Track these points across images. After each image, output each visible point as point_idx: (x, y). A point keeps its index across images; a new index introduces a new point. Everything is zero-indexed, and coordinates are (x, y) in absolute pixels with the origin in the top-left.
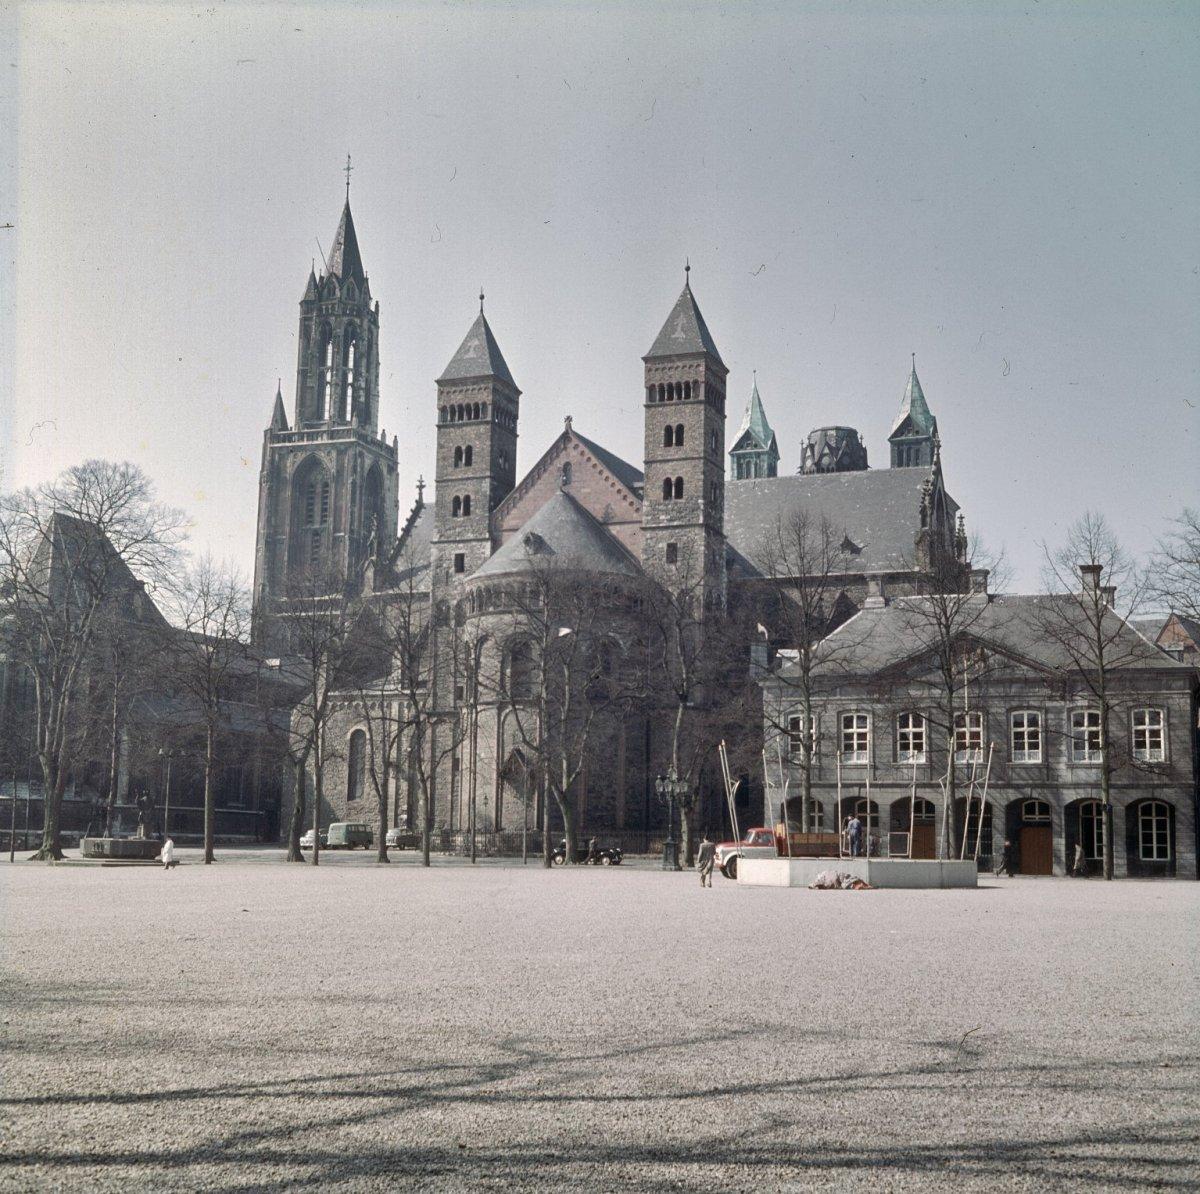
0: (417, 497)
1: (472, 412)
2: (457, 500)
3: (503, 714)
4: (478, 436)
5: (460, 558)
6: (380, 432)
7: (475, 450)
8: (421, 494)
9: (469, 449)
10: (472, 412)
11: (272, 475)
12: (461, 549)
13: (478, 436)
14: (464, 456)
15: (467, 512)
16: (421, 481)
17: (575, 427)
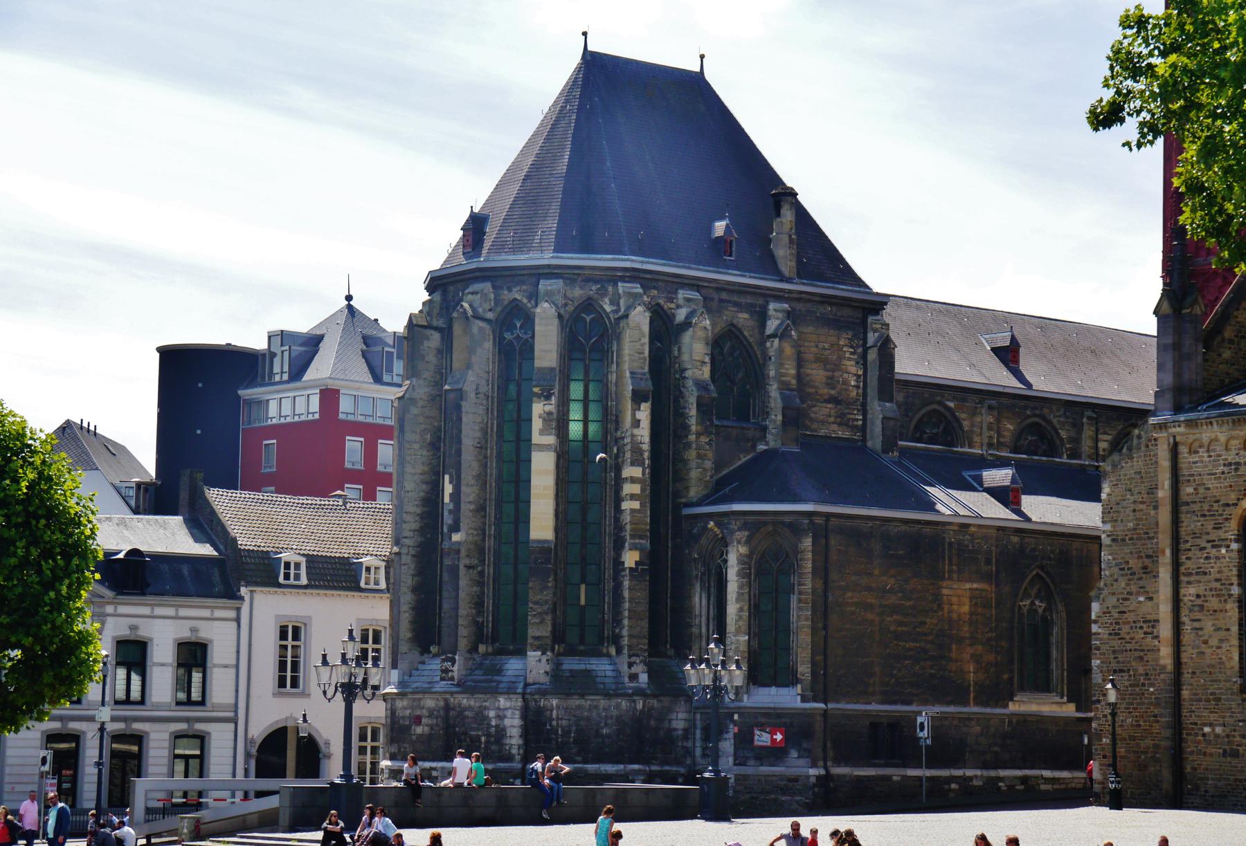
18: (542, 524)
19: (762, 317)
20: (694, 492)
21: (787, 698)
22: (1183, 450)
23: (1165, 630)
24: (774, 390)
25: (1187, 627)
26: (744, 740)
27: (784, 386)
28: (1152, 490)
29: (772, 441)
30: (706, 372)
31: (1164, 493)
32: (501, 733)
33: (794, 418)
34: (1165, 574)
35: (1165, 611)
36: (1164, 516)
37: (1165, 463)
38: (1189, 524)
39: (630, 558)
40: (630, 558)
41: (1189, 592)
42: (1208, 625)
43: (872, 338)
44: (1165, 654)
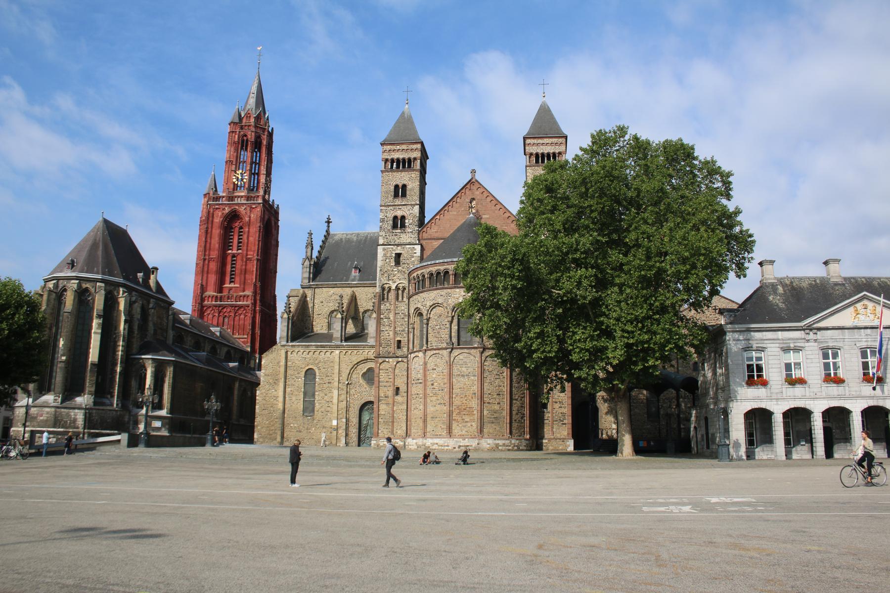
0: (326, 228)
1: (404, 164)
2: (395, 218)
3: (453, 355)
4: (410, 179)
5: (398, 255)
6: (271, 200)
7: (409, 187)
8: (328, 226)
9: (404, 186)
10: (404, 164)
11: (207, 221)
12: (399, 250)
13: (410, 179)
14: (400, 191)
15: (403, 226)
16: (329, 219)
17: (478, 177)
18: (94, 355)
19: (149, 303)
20: (134, 351)
21: (163, 413)
22: (289, 353)
23: (281, 399)
24: (151, 325)
25: (287, 399)
26: (147, 424)
27: (154, 324)
28: (278, 363)
29: (149, 338)
30: (139, 317)
31: (283, 363)
32: (75, 420)
33: (155, 333)
34: (282, 385)
35: (281, 394)
36: (282, 369)
37: (283, 355)
38: (289, 372)
39: (118, 369)
40: (118, 369)
41: (288, 390)
42: (294, 398)
43: (170, 312)
44: (280, 406)
